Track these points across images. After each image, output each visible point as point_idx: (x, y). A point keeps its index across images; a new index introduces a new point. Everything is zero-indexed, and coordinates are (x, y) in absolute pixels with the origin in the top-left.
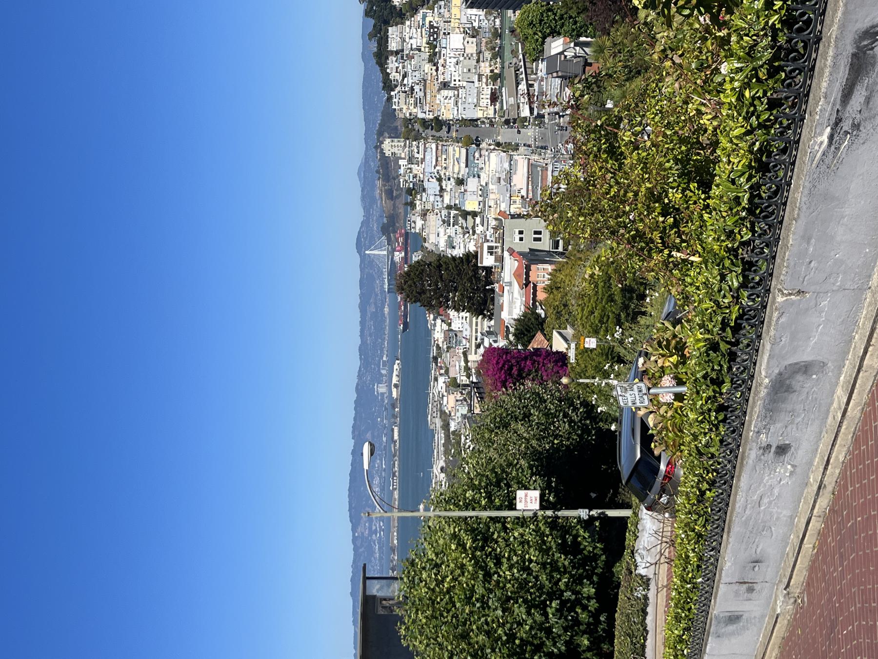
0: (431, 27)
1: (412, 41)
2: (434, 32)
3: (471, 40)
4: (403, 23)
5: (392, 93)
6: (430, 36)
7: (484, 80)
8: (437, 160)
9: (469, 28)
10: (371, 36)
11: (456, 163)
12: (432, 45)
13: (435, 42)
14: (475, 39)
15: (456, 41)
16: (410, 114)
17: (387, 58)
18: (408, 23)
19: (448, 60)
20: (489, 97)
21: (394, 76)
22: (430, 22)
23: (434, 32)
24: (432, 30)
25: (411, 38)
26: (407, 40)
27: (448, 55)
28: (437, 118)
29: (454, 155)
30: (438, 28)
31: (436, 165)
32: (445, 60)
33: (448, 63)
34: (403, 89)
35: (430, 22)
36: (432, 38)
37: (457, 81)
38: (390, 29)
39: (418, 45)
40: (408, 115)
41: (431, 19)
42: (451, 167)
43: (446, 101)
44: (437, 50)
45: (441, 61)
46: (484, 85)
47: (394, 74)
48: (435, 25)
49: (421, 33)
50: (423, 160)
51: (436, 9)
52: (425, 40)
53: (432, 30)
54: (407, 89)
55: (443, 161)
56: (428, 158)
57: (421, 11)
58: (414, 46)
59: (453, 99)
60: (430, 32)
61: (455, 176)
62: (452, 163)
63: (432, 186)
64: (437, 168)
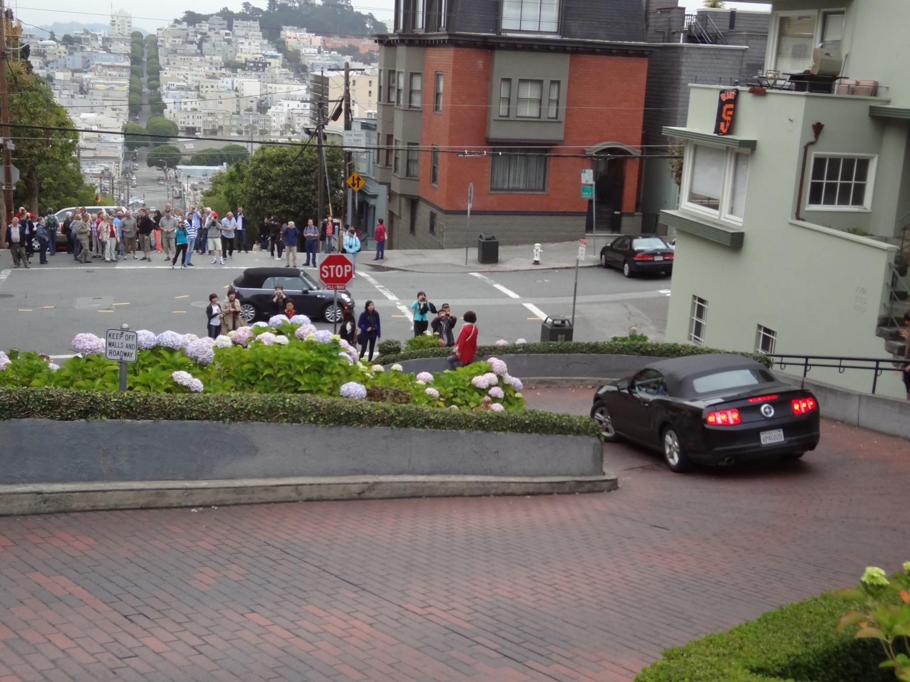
0: (265, 65)
1: (246, 43)
2: (258, 66)
3: (254, 106)
4: (264, 37)
5: (185, 24)
6: (254, 62)
7: (210, 119)
8: (109, 67)
9: (267, 104)
10: (246, 5)
11: (107, 87)
12: (243, 66)
13: (247, 69)
14: (255, 107)
15: (251, 86)
16: (162, 41)
17: (224, 19)
18: (266, 42)
19: (229, 80)
20: (191, 125)
21: (205, 27)
22: (270, 64)
23: (258, 66)
24: (260, 65)
25: (250, 44)
26: (249, 41)
27: (235, 79)
28: (161, 69)
29: (117, 84)
30: (264, 71)
31: (103, 66)
32: (229, 76)
33: (226, 79)
34: (190, 34)
35: (270, 64)
36: (252, 65)
37: (207, 89)
38: (257, 24)
39: (243, 50)
40: (162, 39)
41: (273, 65)
42: (101, 81)
43: (182, 77)
44: (239, 70)
45: (228, 72)
46: (205, 119)
47: (208, 25)
48: (266, 69)
49: (257, 54)
50: (109, 51)
51: (284, 70)
52: (250, 57)
53: (260, 65)
54: (190, 37)
55: (109, 72)
56: (112, 57)
57: (280, 55)
58: (241, 46)
59: (185, 84)
60: (259, 63)
61: (91, 86)
62: (107, 82)
63: (77, 60)
64: (100, 67)
